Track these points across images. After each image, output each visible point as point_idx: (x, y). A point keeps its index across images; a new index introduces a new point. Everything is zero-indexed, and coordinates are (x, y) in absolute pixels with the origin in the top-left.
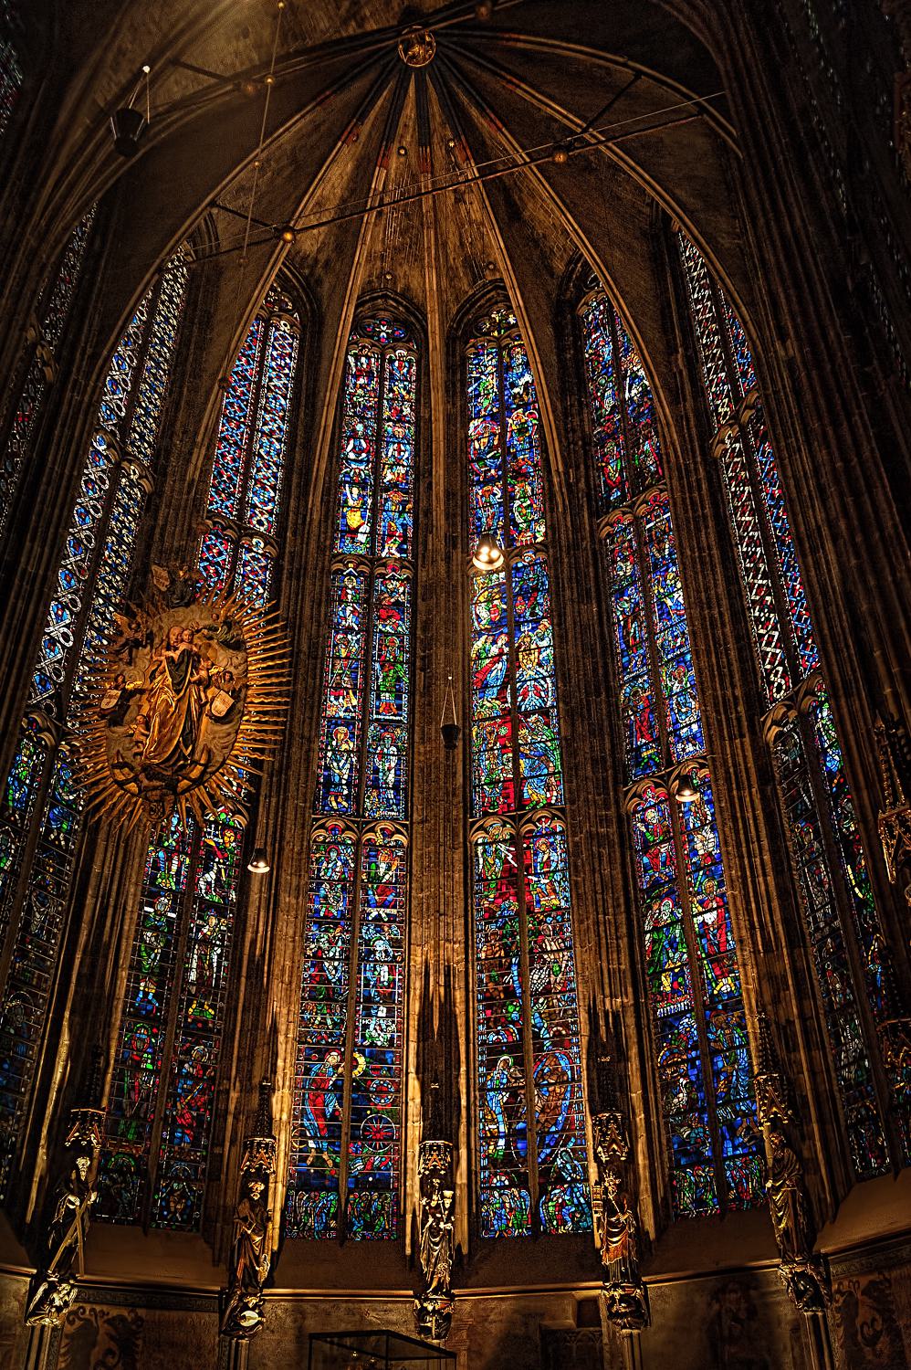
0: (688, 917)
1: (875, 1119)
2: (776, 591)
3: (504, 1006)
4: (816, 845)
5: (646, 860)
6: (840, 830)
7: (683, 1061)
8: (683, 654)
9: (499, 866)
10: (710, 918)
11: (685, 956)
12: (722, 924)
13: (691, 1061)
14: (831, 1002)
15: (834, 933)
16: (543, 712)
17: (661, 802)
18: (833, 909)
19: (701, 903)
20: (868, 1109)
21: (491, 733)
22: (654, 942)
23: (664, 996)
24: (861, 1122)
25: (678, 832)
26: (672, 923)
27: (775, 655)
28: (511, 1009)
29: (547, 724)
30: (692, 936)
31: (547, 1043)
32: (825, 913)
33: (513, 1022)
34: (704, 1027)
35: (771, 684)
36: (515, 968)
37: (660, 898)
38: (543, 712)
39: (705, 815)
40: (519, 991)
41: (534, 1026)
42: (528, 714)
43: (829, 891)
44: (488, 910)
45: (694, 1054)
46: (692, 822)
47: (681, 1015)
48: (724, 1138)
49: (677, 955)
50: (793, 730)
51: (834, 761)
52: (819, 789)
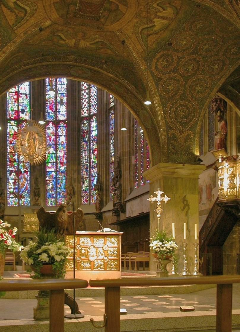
0: (56, 153)
1: (87, 196)
2: (90, 90)
3: (13, 163)
4: (86, 148)
5: (48, 139)
6: (92, 147)
7: (51, 180)
8: (63, 93)
9: (13, 132)
10: (62, 155)
11: (55, 161)
12: (64, 156)
13: (54, 180)
14: (83, 176)
15: (86, 165)
16: (26, 95)
17: (53, 127)
18: (87, 161)
19: (60, 151)
20: (86, 194)
21: (12, 96)
22: (48, 156)
23: (49, 168)
24: (85, 196)
25: (57, 135)
26: (52, 154)
27: (85, 105)
28: (15, 164)
29: (27, 98)
30: (56, 158)
31: (23, 172)
32: (85, 161)
33: (15, 166)
34: (57, 175)
35: (83, 111)
36: (16, 155)
37: (50, 147)
38: (26, 95)
39: (63, 133)
40: (17, 160)
41: (20, 168)
42: (22, 94)
43: (87, 157)
44: (10, 141)
45: (54, 179)
46: (60, 134)
47: (52, 172)
48: (58, 194)
49: (53, 160)
50: (87, 123)
51: (94, 133)
52: (89, 137)
